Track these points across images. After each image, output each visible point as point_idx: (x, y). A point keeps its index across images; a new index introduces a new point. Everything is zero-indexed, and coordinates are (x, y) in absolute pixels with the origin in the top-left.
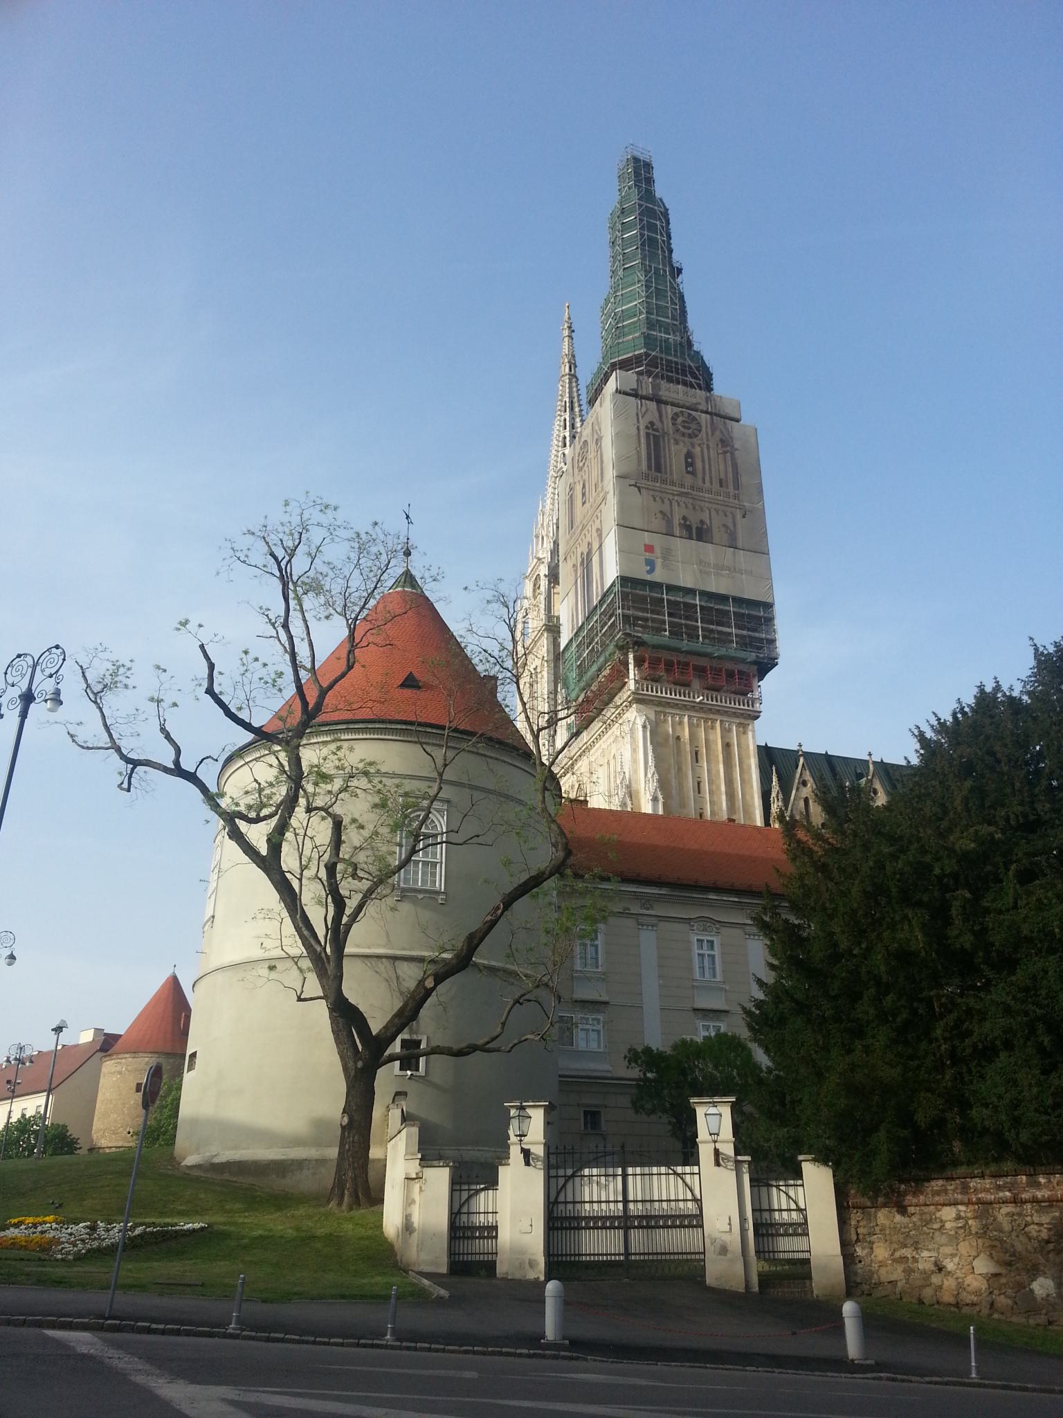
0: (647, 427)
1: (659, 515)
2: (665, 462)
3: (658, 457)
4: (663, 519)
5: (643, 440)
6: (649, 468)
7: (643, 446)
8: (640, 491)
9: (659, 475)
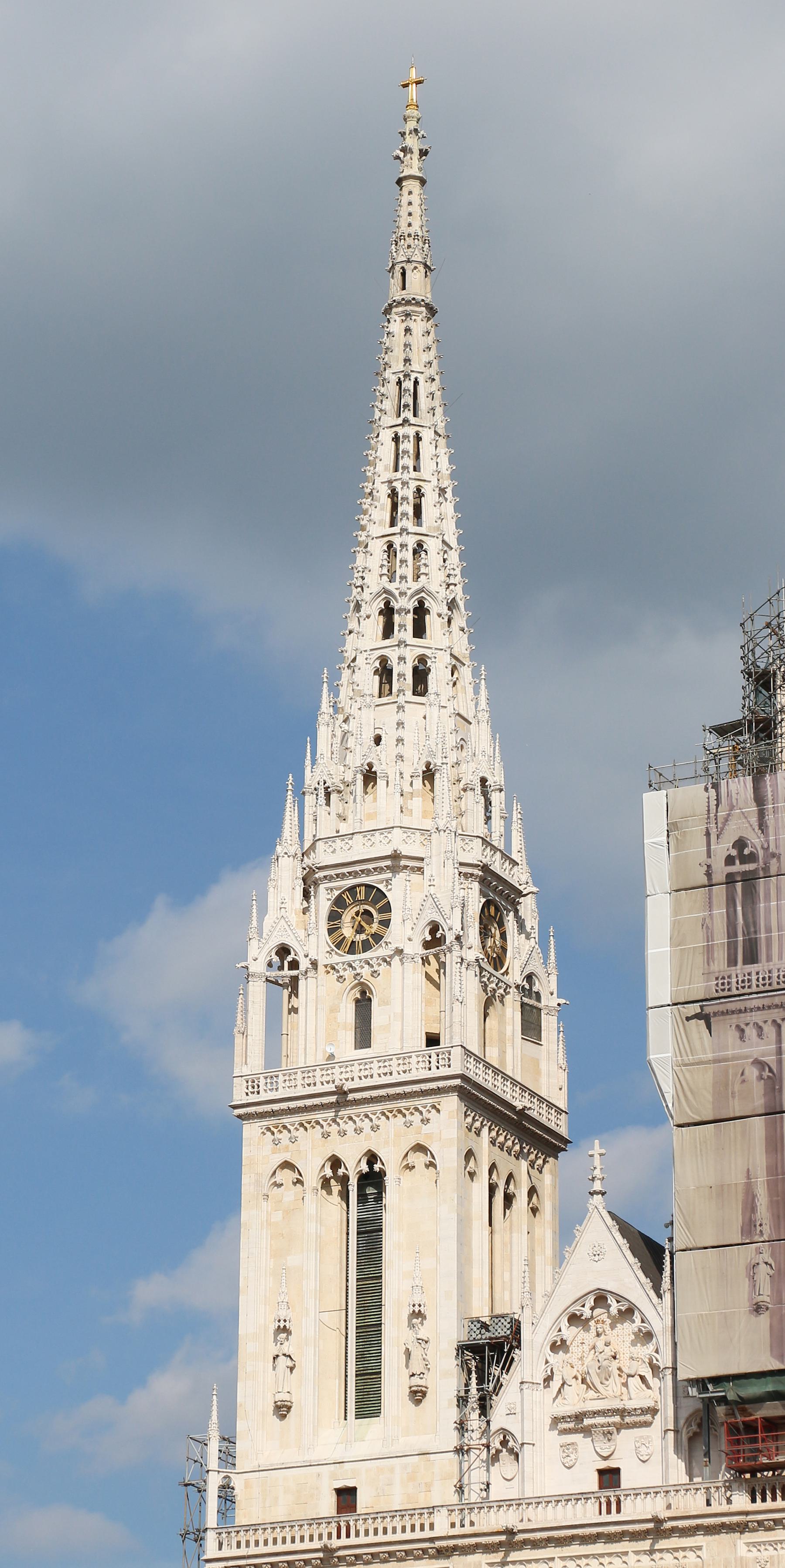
0: (730, 860)
1: (753, 1073)
2: (769, 930)
3: (751, 924)
4: (760, 1078)
5: (720, 892)
6: (732, 962)
7: (720, 912)
8: (709, 1027)
9: (753, 968)
